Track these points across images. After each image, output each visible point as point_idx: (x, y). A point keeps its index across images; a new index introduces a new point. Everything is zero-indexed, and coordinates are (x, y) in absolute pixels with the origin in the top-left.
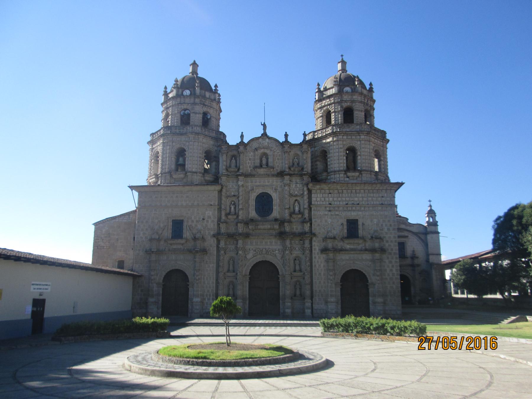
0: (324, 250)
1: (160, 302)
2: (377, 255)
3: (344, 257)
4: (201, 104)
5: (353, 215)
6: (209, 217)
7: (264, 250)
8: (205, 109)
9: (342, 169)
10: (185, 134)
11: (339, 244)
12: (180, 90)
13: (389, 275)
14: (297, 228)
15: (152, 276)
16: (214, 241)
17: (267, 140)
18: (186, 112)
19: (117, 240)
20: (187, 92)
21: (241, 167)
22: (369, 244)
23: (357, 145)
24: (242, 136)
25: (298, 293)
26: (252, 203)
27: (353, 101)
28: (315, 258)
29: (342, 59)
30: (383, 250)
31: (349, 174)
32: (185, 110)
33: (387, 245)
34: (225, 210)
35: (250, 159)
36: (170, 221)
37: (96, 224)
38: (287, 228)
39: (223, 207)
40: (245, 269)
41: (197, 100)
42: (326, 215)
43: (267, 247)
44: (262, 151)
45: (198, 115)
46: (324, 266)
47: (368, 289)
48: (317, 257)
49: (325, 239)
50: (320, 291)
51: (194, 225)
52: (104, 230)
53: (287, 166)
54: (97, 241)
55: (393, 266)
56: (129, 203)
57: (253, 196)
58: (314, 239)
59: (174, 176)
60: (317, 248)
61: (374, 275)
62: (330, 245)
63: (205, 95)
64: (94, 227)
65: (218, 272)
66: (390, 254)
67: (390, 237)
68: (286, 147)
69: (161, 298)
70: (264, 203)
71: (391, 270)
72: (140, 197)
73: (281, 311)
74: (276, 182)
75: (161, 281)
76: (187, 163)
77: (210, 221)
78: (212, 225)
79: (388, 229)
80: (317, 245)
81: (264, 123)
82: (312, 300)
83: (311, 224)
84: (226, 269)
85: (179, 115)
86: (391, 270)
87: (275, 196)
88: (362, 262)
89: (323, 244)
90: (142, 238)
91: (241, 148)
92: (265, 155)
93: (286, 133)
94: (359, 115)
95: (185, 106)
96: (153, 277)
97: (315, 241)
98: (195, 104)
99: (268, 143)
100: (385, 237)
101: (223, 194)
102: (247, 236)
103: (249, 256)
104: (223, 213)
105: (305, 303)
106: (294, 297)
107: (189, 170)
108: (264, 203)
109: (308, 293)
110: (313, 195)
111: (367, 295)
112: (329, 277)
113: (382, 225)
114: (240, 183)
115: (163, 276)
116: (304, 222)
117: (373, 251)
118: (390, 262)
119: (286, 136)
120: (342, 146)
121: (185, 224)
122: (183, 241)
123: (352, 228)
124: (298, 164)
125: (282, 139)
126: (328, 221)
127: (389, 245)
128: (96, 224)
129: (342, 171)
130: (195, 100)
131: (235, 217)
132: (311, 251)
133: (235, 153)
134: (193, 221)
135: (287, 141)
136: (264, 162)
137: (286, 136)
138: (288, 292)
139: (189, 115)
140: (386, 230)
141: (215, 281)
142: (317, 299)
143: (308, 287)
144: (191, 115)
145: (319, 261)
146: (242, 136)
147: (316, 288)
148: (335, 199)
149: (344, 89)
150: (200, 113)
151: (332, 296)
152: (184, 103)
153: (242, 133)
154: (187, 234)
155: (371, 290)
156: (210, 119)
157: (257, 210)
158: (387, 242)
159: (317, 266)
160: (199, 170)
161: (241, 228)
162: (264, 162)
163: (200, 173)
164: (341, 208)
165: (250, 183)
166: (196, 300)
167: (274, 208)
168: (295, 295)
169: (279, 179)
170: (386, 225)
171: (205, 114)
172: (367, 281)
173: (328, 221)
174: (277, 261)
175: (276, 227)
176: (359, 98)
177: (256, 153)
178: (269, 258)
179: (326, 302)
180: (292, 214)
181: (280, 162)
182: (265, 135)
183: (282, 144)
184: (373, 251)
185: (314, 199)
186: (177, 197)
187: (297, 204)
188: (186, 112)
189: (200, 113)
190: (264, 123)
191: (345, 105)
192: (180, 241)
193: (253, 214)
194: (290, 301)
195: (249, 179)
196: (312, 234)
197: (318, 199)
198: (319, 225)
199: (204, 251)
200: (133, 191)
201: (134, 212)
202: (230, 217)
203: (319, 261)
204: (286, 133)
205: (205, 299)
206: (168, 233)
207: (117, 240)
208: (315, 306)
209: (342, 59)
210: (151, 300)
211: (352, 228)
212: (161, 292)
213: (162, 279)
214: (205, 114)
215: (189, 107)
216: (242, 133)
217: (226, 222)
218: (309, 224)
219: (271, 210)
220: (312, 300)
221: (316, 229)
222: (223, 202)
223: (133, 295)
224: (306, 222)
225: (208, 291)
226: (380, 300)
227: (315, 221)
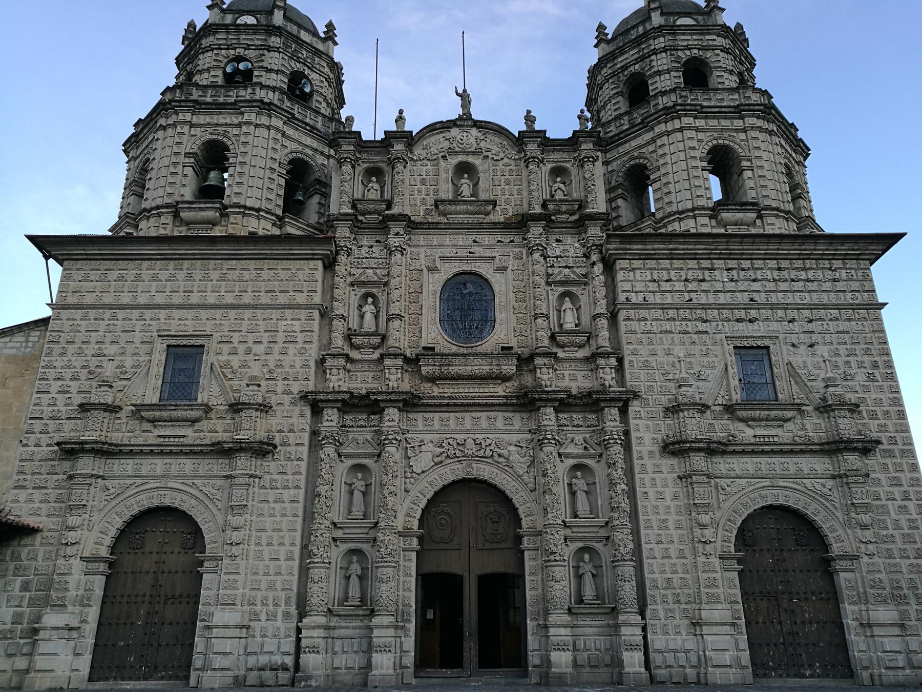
1: (91, 628)
2: (852, 460)
7: (470, 442)
13: (898, 527)
16: (302, 416)
17: (474, 132)
18: (241, 66)
21: (396, 200)
22: (814, 428)
23: (738, 142)
24: (400, 119)
25: (589, 591)
26: (431, 301)
28: (643, 467)
31: (725, 215)
32: (239, 59)
33: (873, 424)
35: (423, 182)
36: (160, 347)
40: (405, 508)
41: (275, 41)
42: (666, 332)
44: (460, 158)
46: (675, 497)
47: (830, 575)
48: (650, 468)
49: (674, 410)
50: (669, 583)
51: (235, 362)
55: (906, 496)
57: (433, 284)
58: (635, 407)
60: (647, 438)
61: (848, 524)
65: (309, 516)
66: (889, 454)
67: (878, 402)
68: (532, 147)
69: (93, 613)
70: (467, 301)
71: (903, 509)
72: (65, 278)
73: (534, 659)
75: (104, 552)
79: (871, 378)
80: (647, 429)
81: (465, 91)
82: (643, 618)
87: (498, 282)
88: (803, 483)
89: (666, 428)
91: (398, 147)
93: (529, 112)
96: (72, 536)
97: (638, 415)
103: (422, 461)
105: (617, 626)
106: (577, 607)
108: (467, 301)
109: (629, 590)
110: (620, 275)
111: (833, 597)
112: (698, 532)
114: (393, 241)
115: (113, 532)
121: (208, 358)
125: (516, 126)
129: (703, 208)
132: (627, 446)
133: (378, 160)
140: (861, 376)
141: (297, 551)
142: (661, 614)
143: (628, 570)
144: (256, 73)
145: (658, 479)
146: (400, 119)
147: (654, 571)
148: (691, 287)
150: (283, 72)
153: (401, 112)
154: (209, 392)
155: (844, 579)
158: (873, 415)
159: (651, 495)
160: (265, 205)
166: (221, 616)
167: (500, 316)
168: (580, 601)
170: (861, 365)
171: (296, 79)
172: (826, 547)
175: (509, 367)
176: (720, 41)
178: (485, 471)
179: (696, 624)
181: (511, 187)
182: (465, 121)
183: (519, 141)
185: (622, 286)
187: (567, 304)
188: (241, 66)
190: (465, 91)
191: (684, 55)
193: (432, 334)
194: (567, 618)
198: (646, 365)
200: (51, 261)
201: (45, 321)
203: (658, 479)
204: (529, 112)
208: (657, 641)
212: (99, 592)
213: (108, 541)
214: (296, 79)
215: (251, 54)
216: (401, 112)
218: (613, 361)
219: (488, 322)
220: (643, 618)
221: (636, 376)
225: (271, 587)
226: (885, 614)
227: (634, 353)
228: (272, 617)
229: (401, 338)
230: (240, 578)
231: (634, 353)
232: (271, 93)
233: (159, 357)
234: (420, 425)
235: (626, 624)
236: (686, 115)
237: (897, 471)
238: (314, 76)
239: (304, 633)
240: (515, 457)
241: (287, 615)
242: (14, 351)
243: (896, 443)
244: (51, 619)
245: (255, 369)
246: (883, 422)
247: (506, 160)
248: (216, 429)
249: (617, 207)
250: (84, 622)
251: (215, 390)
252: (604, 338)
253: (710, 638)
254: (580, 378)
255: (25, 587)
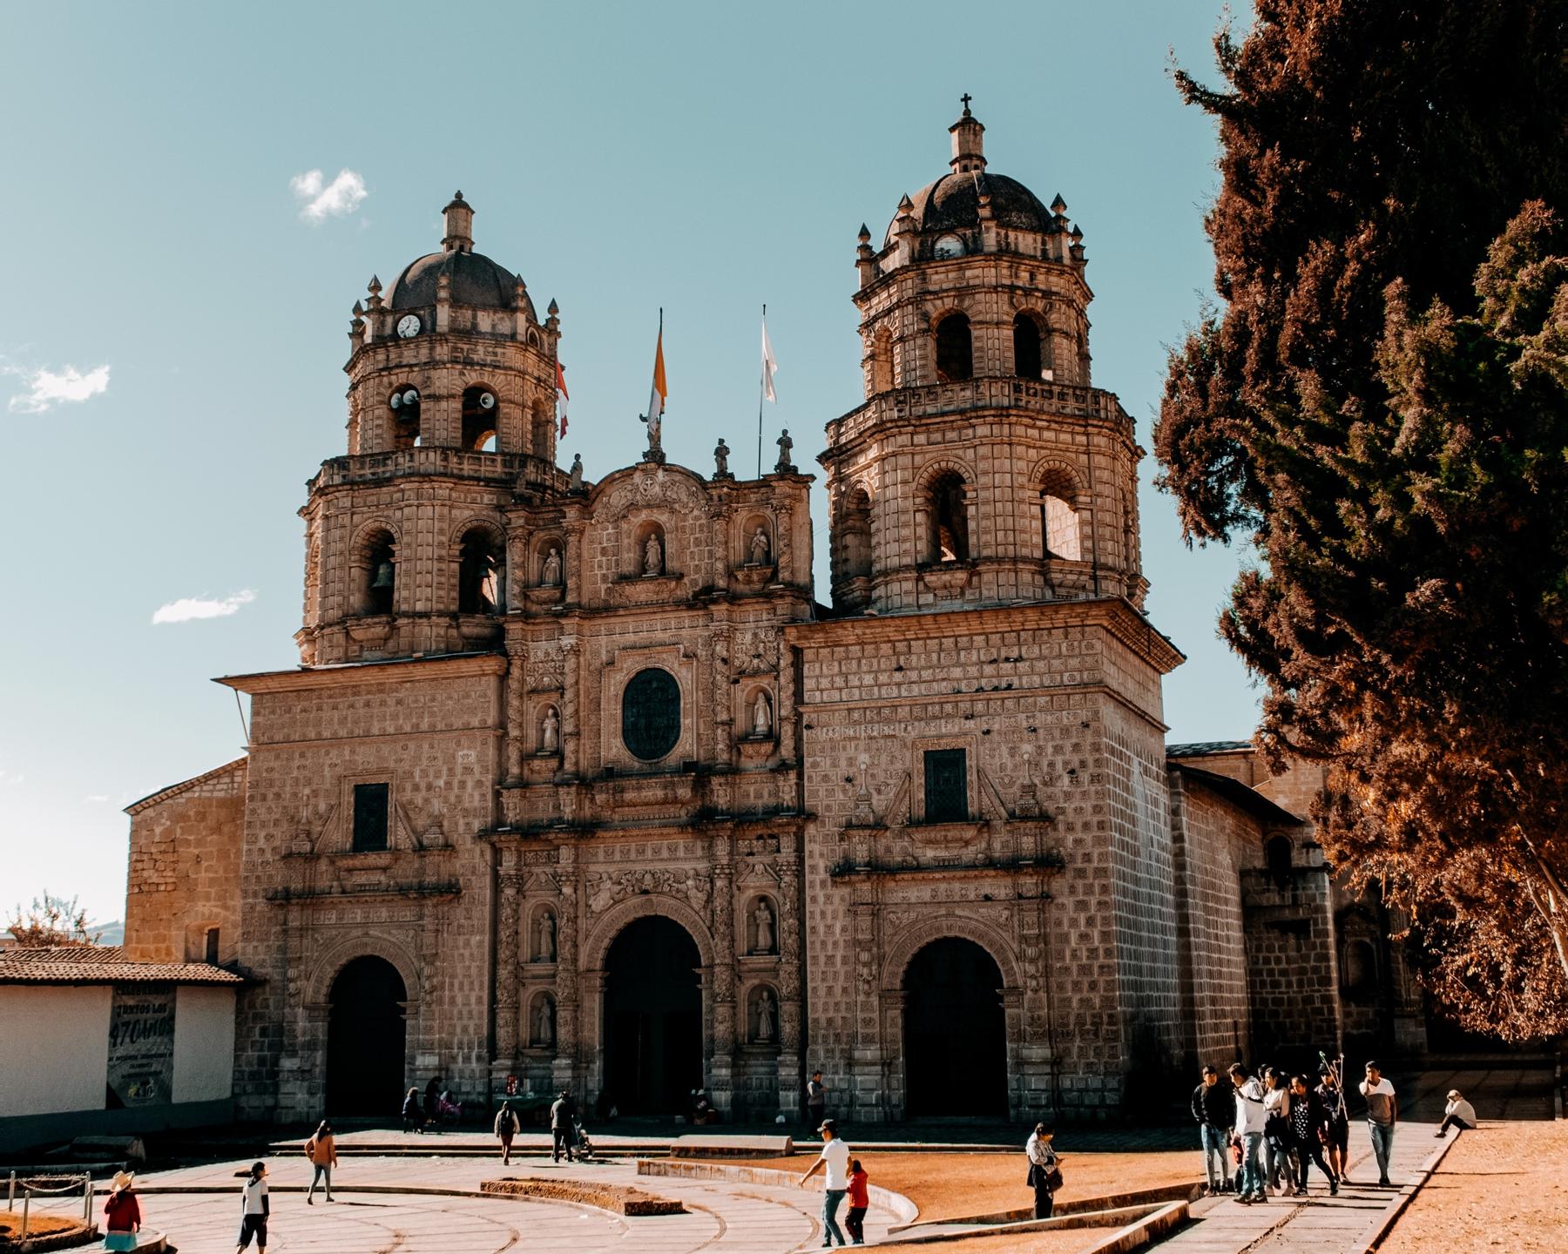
0: (843, 871)
2: (1029, 883)
3: (913, 892)
4: (455, 361)
5: (946, 732)
6: (468, 770)
8: (473, 378)
9: (907, 560)
10: (388, 481)
11: (896, 847)
12: (390, 320)
14: (756, 791)
15: (291, 980)
16: (482, 854)
17: (660, 473)
19: (198, 860)
20: (409, 325)
22: (1000, 844)
23: (963, 460)
26: (612, 712)
27: (963, 291)
28: (814, 899)
29: (967, 112)
30: (1049, 863)
31: (928, 578)
32: (402, 389)
34: (521, 740)
35: (604, 552)
36: (348, 788)
37: (134, 810)
38: (721, 796)
39: (514, 732)
42: (850, 739)
43: (659, 866)
44: (644, 515)
45: (444, 404)
46: (844, 929)
48: (821, 899)
50: (830, 1021)
51: (419, 801)
52: (158, 830)
53: (720, 566)
54: (139, 866)
55: (1090, 922)
56: (221, 736)
57: (616, 684)
58: (811, 830)
59: (358, 634)
60: (821, 864)
62: (861, 853)
63: (475, 326)
64: (127, 818)
66: (1081, 873)
67: (1079, 810)
70: (652, 704)
72: (255, 713)
74: (688, 628)
76: (397, 582)
77: (470, 784)
78: (477, 798)
80: (820, 853)
83: (800, 776)
84: (525, 952)
85: (382, 411)
86: (1084, 937)
87: (685, 677)
89: (839, 849)
90: (262, 851)
92: (657, 530)
93: (721, 441)
94: (994, 344)
95: (401, 378)
98: (433, 364)
99: (663, 485)
100: (1062, 811)
101: (514, 685)
102: (585, 830)
103: (600, 902)
104: (513, 753)
107: (404, 607)
108: (652, 704)
113: (1051, 765)
116: (782, 768)
117: (1011, 866)
118: (1082, 905)
119: (722, 452)
120: (908, 475)
121: (392, 798)
122: (383, 859)
123: (945, 782)
124: (768, 553)
126: (857, 759)
127: (1078, 842)
128: (134, 810)
130: (432, 349)
131: (554, 763)
132: (800, 874)
134: (416, 788)
135: (723, 475)
136: (652, 558)
137: (722, 452)
138: (721, 1030)
139: (415, 405)
142: (822, 1053)
144: (423, 406)
145: (829, 912)
147: (818, 1009)
148: (883, 678)
149: (938, 246)
150: (453, 396)
151: (868, 1040)
152: (399, 366)
153: (577, 457)
154: (399, 835)
156: (496, 407)
157: (631, 735)
158: (1070, 828)
159: (821, 929)
161: (569, 805)
162: (652, 558)
163: (440, 614)
164: (903, 712)
165: (605, 639)
167: (686, 722)
169: (699, 617)
173: (857, 759)
174: (690, 916)
175: (684, 792)
177: (624, 526)
178: (665, 906)
179: (851, 1063)
180: (737, 742)
182: (655, 456)
184: (1011, 866)
185: (809, 684)
186: (367, 704)
187: (761, 702)
188: (408, 395)
189: (453, 396)
191: (935, 308)
192: (373, 859)
193: (614, 749)
195: (601, 624)
196: (803, 815)
197: (825, 683)
199: (451, 890)
202: (536, 764)
205: (454, 1058)
206: (340, 834)
207: (198, 860)
209: (967, 112)
210: (288, 1064)
211: (945, 782)
215: (415, 377)
216: (577, 457)
217: (523, 784)
218: (792, 776)
222: (511, 713)
223: (239, 1048)
224: (791, 768)
225: (465, 1029)
226: (1038, 1052)
228: (467, 1059)
229: (577, 756)
230: (436, 1024)
231: (815, 765)
232: (432, 455)
233: (349, 799)
234: (601, 857)
235: (782, 1064)
236: (900, 433)
237: (1085, 894)
238: (498, 381)
239: (494, 1075)
240: (692, 893)
241: (479, 1058)
242: (222, 794)
243: (1089, 861)
244: (288, 1064)
245: (437, 806)
246: (1080, 835)
247: (696, 512)
248: (406, 871)
249: (846, 547)
250: (314, 1065)
251: (402, 833)
252: (787, 750)
253: (859, 1078)
254: (766, 795)
255: (264, 1032)
